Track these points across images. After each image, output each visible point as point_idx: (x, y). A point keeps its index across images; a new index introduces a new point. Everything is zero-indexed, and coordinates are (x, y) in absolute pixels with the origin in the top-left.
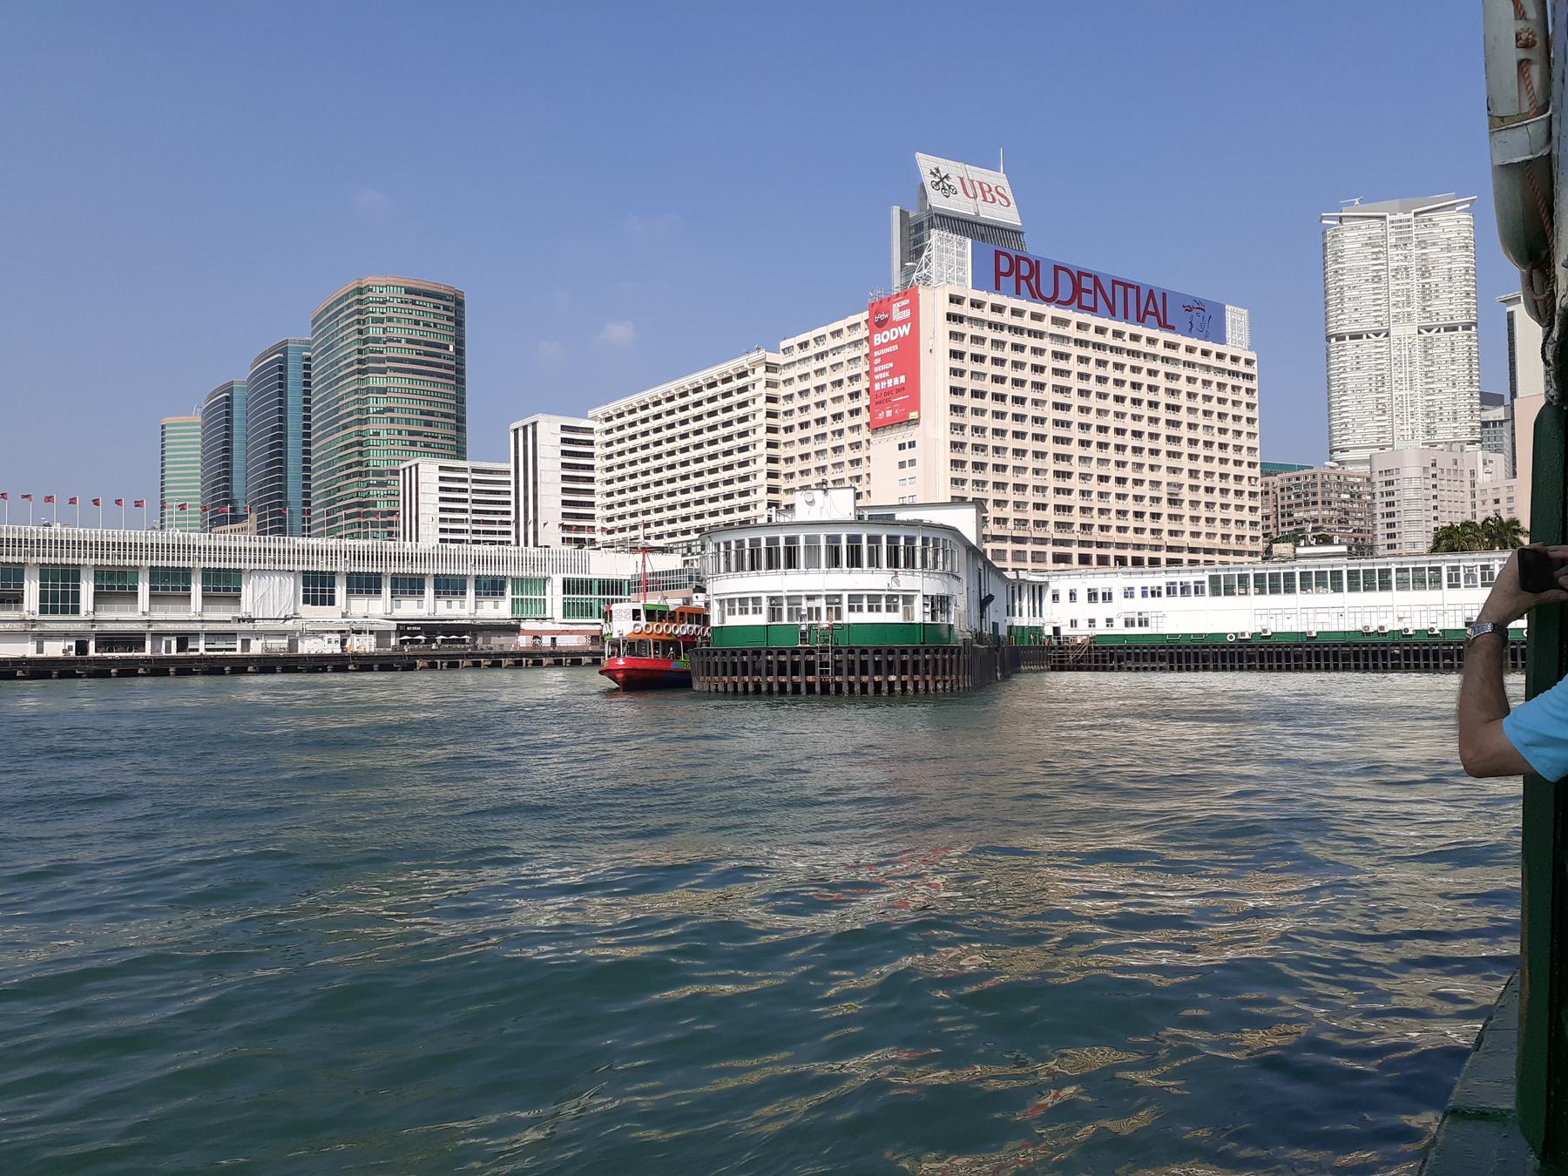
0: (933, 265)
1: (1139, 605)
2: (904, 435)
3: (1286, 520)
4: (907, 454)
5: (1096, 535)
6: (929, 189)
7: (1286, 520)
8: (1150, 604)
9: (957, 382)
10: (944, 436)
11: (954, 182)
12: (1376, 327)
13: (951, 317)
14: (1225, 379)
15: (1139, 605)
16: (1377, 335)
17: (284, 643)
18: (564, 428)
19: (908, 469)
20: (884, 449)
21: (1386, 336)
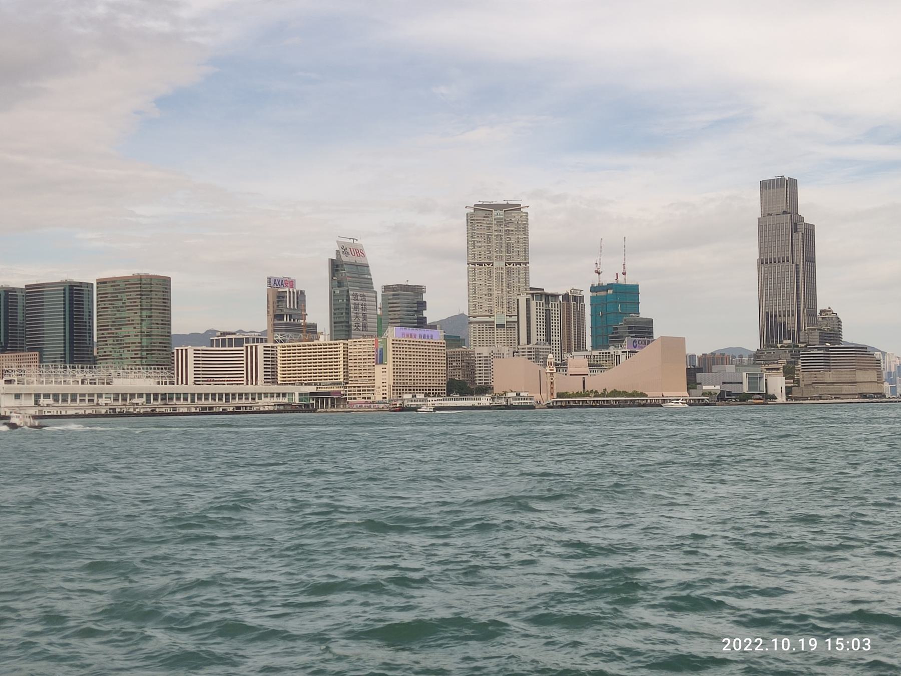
0: (389, 333)
1: (433, 402)
2: (384, 366)
3: (451, 365)
4: (384, 370)
5: (416, 385)
6: (341, 254)
7: (451, 365)
8: (435, 402)
9: (394, 356)
10: (392, 367)
11: (348, 250)
12: (488, 261)
13: (393, 344)
14: (440, 348)
15: (433, 402)
16: (489, 265)
17: (258, 408)
18: (264, 347)
19: (384, 373)
20: (378, 368)
21: (492, 265)
